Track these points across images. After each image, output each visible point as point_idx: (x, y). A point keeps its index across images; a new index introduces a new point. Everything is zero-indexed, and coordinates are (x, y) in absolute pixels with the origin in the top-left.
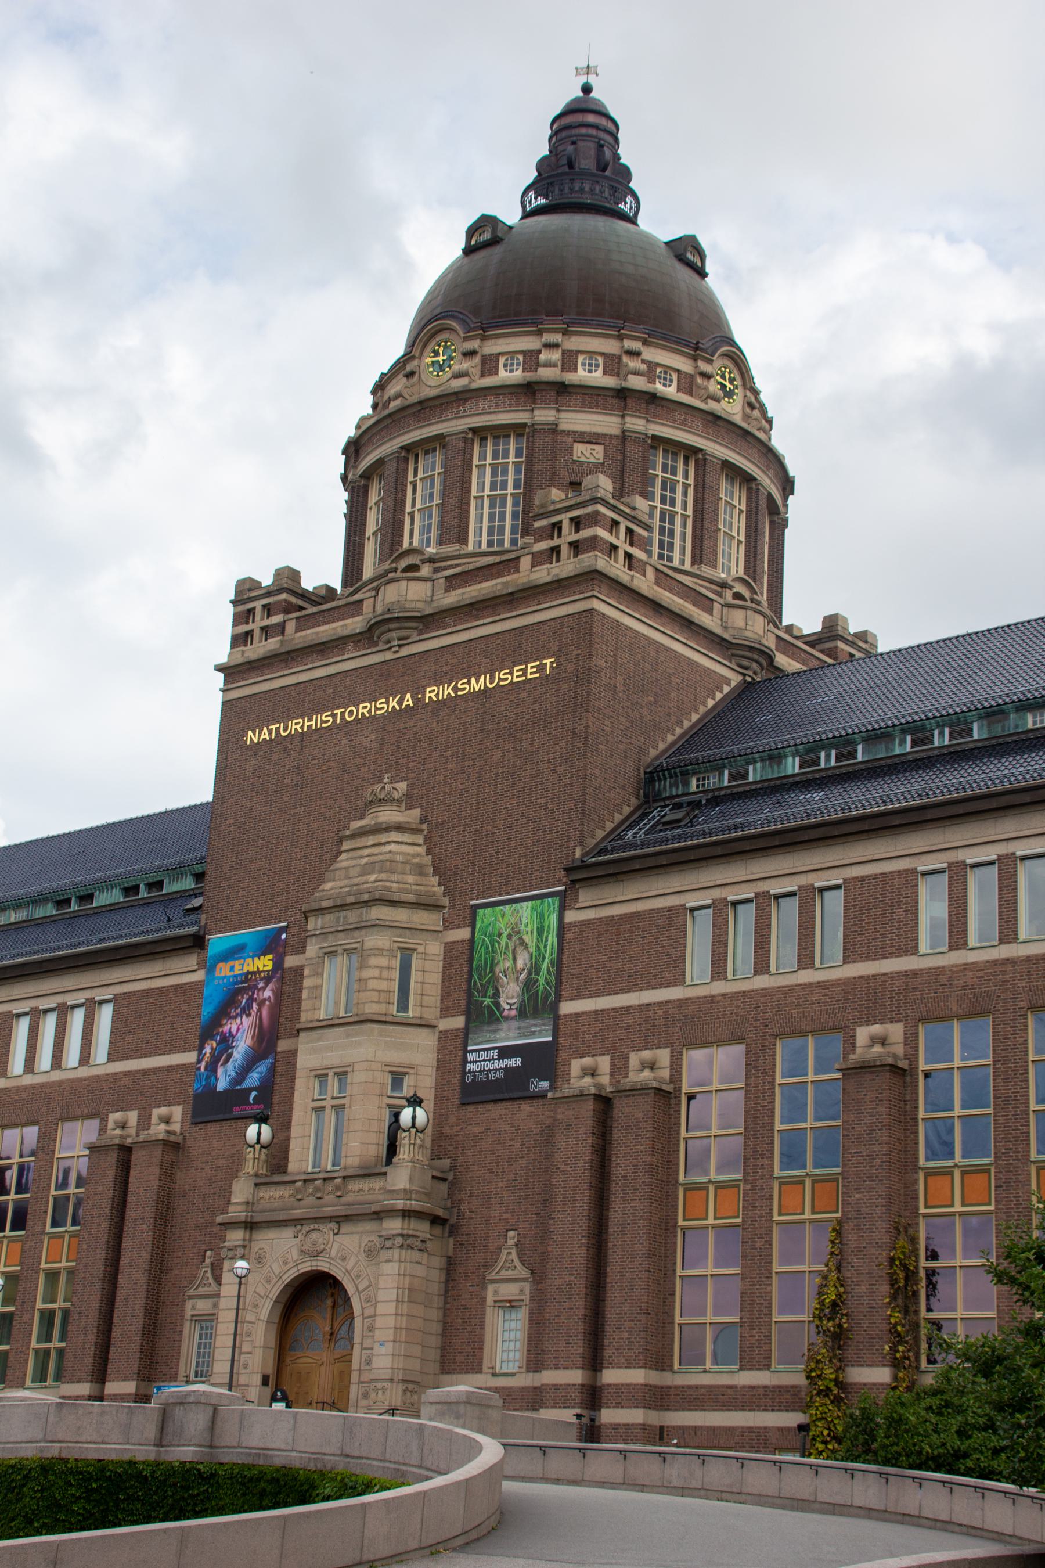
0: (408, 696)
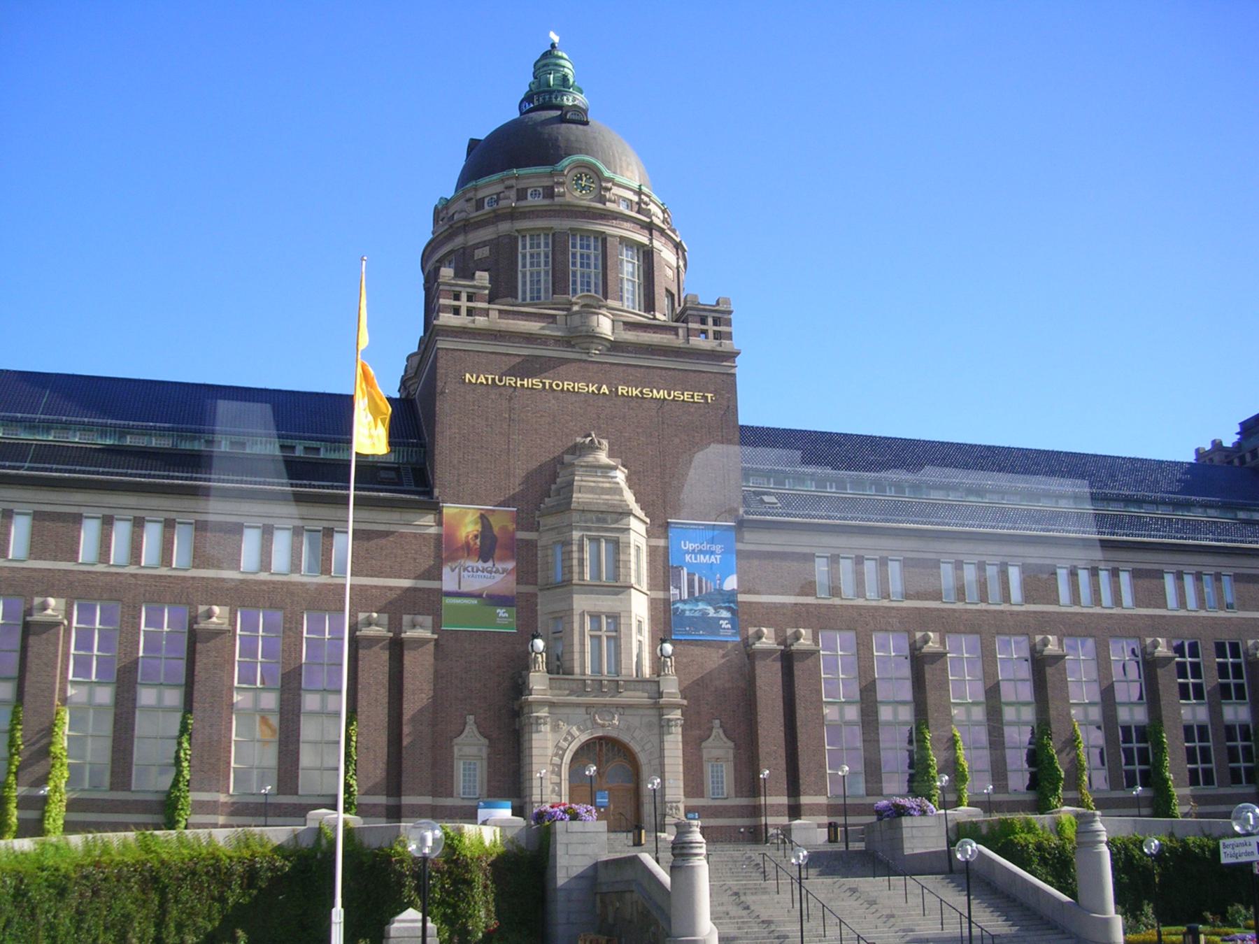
0: (604, 387)
